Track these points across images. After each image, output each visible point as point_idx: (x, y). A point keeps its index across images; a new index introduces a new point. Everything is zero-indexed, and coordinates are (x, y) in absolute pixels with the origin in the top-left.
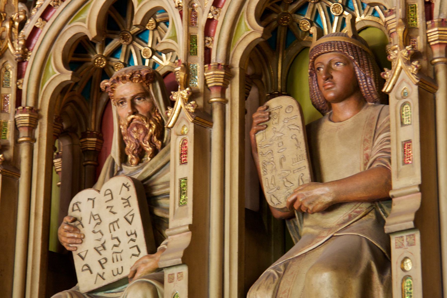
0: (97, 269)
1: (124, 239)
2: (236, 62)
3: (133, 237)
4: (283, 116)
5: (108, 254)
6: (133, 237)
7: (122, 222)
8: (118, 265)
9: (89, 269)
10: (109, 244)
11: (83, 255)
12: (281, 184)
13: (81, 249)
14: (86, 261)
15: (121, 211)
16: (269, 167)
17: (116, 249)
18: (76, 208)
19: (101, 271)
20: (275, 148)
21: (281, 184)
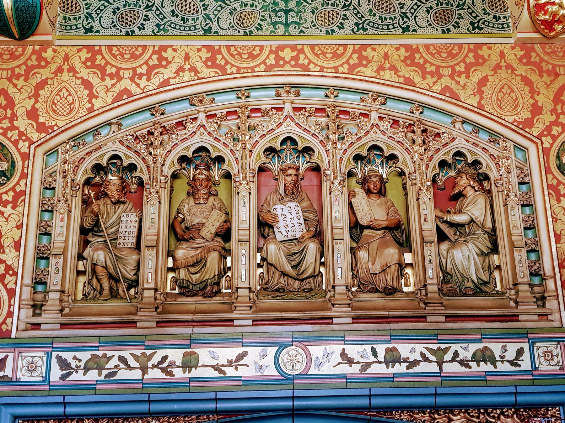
0: (285, 233)
1: (297, 225)
2: (346, 173)
3: (300, 225)
4: (360, 195)
5: (289, 229)
6: (300, 225)
7: (295, 218)
8: (294, 233)
9: (281, 233)
10: (290, 226)
11: (278, 227)
12: (364, 218)
13: (278, 225)
14: (279, 230)
15: (295, 215)
16: (358, 211)
17: (293, 228)
18: (275, 210)
19: (287, 235)
20: (360, 206)
21: (364, 218)
